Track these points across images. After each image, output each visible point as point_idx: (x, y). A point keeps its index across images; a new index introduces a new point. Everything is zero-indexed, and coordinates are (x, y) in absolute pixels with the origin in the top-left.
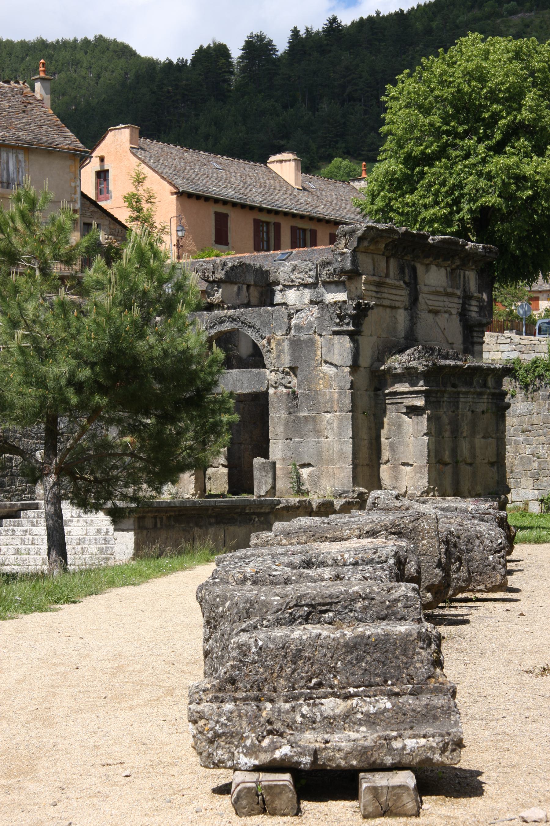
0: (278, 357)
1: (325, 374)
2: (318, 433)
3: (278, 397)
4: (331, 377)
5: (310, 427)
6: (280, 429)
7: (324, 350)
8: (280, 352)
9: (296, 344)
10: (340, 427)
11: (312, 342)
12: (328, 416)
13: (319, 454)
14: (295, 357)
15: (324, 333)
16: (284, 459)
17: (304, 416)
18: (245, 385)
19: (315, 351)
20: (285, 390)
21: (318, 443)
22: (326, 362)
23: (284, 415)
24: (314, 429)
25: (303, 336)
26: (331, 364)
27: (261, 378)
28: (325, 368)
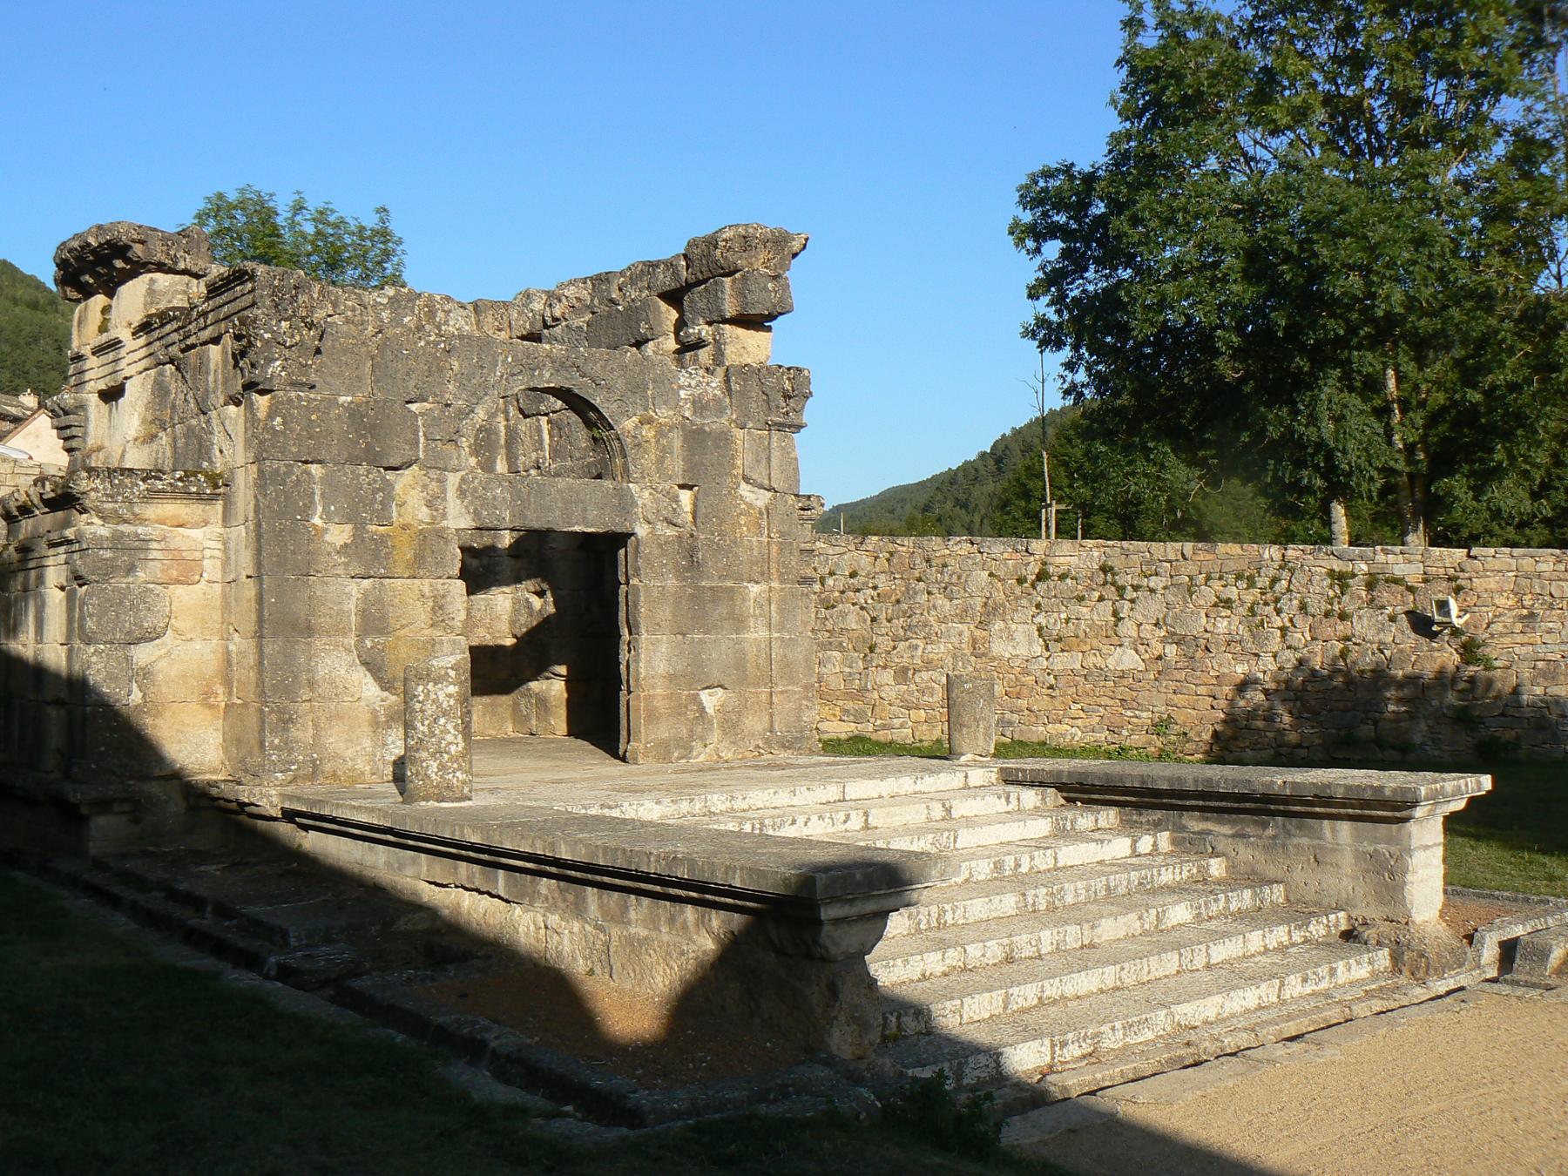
0: (660, 461)
1: (750, 505)
2: (739, 623)
3: (660, 545)
4: (761, 513)
5: (723, 610)
6: (665, 614)
7: (750, 458)
8: (665, 451)
9: (696, 439)
10: (781, 611)
11: (724, 439)
12: (754, 589)
13: (740, 664)
14: (691, 467)
15: (750, 425)
16: (671, 678)
17: (711, 588)
18: (592, 514)
19: (733, 457)
20: (671, 532)
21: (738, 642)
22: (747, 479)
23: (672, 583)
24: (731, 615)
25: (712, 423)
26: (761, 487)
27: (625, 503)
28: (744, 489)
